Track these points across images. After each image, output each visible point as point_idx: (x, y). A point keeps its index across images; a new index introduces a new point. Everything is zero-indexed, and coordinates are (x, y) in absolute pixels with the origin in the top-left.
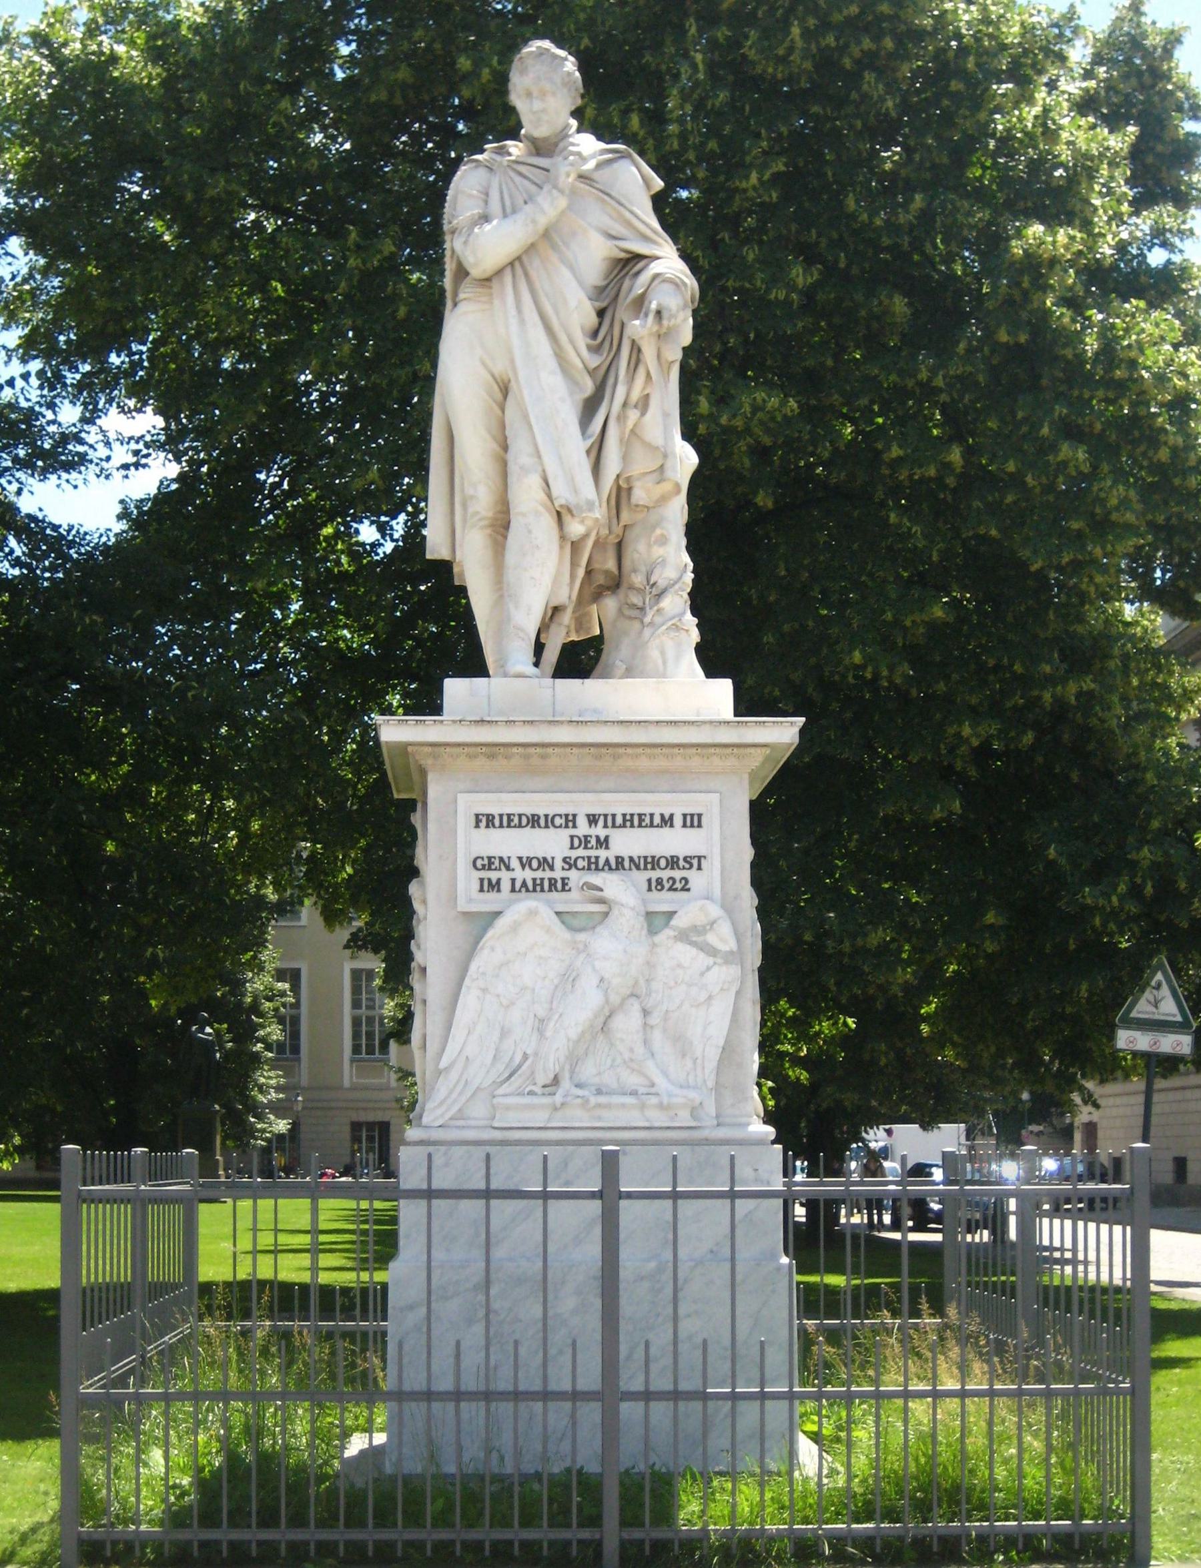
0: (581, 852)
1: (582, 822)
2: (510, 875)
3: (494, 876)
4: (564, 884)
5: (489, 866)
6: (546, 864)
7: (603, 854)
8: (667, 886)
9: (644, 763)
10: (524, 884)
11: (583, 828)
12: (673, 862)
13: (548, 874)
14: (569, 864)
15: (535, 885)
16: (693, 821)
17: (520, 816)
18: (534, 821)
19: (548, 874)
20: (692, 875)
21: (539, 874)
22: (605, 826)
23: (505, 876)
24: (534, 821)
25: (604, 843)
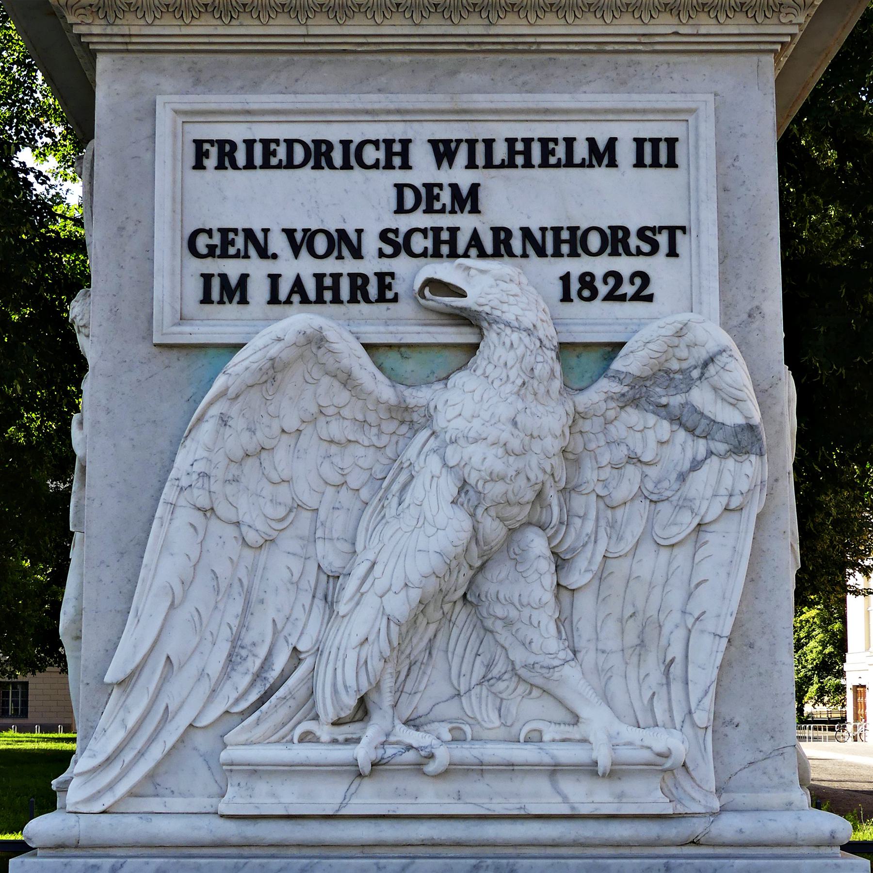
0: (420, 220)
2: (273, 267)
3: (233, 269)
4: (383, 287)
6: (344, 242)
7: (465, 222)
8: (603, 290)
10: (298, 285)
11: (424, 169)
12: (615, 240)
13: (348, 266)
14: (396, 243)
15: (320, 288)
16: (658, 154)
17: (290, 143)
18: (319, 155)
19: (348, 266)
20: (656, 266)
21: (330, 266)
22: (471, 165)
23: (257, 270)
24: (319, 155)
25: (468, 200)
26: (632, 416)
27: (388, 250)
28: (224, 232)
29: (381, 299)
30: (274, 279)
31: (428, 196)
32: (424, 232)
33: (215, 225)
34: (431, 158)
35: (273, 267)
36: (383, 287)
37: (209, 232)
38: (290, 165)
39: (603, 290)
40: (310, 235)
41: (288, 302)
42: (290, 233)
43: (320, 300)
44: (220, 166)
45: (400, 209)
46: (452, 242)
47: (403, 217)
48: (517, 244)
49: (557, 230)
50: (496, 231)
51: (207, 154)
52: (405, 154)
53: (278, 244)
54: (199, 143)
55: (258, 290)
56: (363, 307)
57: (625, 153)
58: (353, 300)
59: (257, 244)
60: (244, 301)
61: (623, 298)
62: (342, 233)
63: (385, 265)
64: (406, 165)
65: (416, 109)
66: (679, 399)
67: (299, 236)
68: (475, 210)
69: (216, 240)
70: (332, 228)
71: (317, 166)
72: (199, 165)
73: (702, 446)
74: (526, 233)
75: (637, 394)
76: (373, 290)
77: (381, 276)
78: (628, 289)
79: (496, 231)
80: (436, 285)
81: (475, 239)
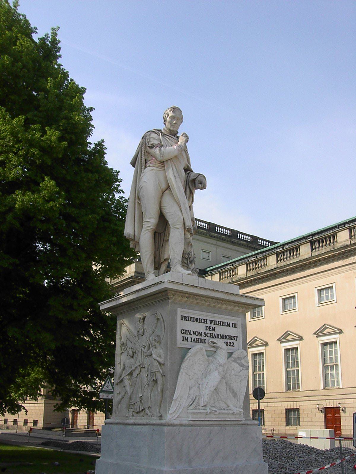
1: (208, 322)
2: (191, 336)
3: (186, 336)
4: (204, 341)
5: (185, 333)
6: (200, 334)
8: (229, 344)
9: (224, 306)
10: (194, 340)
11: (209, 324)
12: (230, 337)
13: (200, 337)
14: (206, 335)
15: (197, 340)
16: (234, 326)
17: (193, 318)
18: (196, 320)
19: (200, 337)
20: (234, 341)
21: (198, 337)
22: (214, 324)
23: (189, 336)
24: (196, 320)
25: (214, 329)
26: (234, 363)
27: (205, 335)
28: (185, 330)
29: (204, 343)
30: (191, 338)
31: (209, 328)
32: (209, 333)
33: (184, 329)
34: (210, 323)
35: (191, 336)
36: (204, 341)
37: (183, 330)
38: (193, 321)
39: (229, 344)
40: (196, 332)
41: (193, 342)
42: (193, 331)
43: (197, 342)
44: (185, 320)
45: (206, 330)
46: (212, 335)
47: (206, 331)
48: (219, 336)
49: (224, 335)
50: (217, 334)
51: (183, 318)
52: (207, 322)
53: (192, 333)
54: (182, 316)
55: (189, 340)
56: (202, 344)
57: (231, 325)
58: (201, 343)
59: (189, 332)
60: (188, 341)
61: (231, 346)
62: (199, 332)
63: (204, 338)
64: (207, 323)
65: (209, 316)
66: (240, 361)
67: (194, 332)
68: (215, 331)
69: (184, 331)
70: (198, 331)
71: (196, 322)
72: (182, 320)
73: (242, 368)
74: (220, 335)
75: (235, 361)
76: (203, 341)
77: (204, 339)
78: (231, 345)
79: (217, 334)
80: (212, 342)
81: (215, 335)
